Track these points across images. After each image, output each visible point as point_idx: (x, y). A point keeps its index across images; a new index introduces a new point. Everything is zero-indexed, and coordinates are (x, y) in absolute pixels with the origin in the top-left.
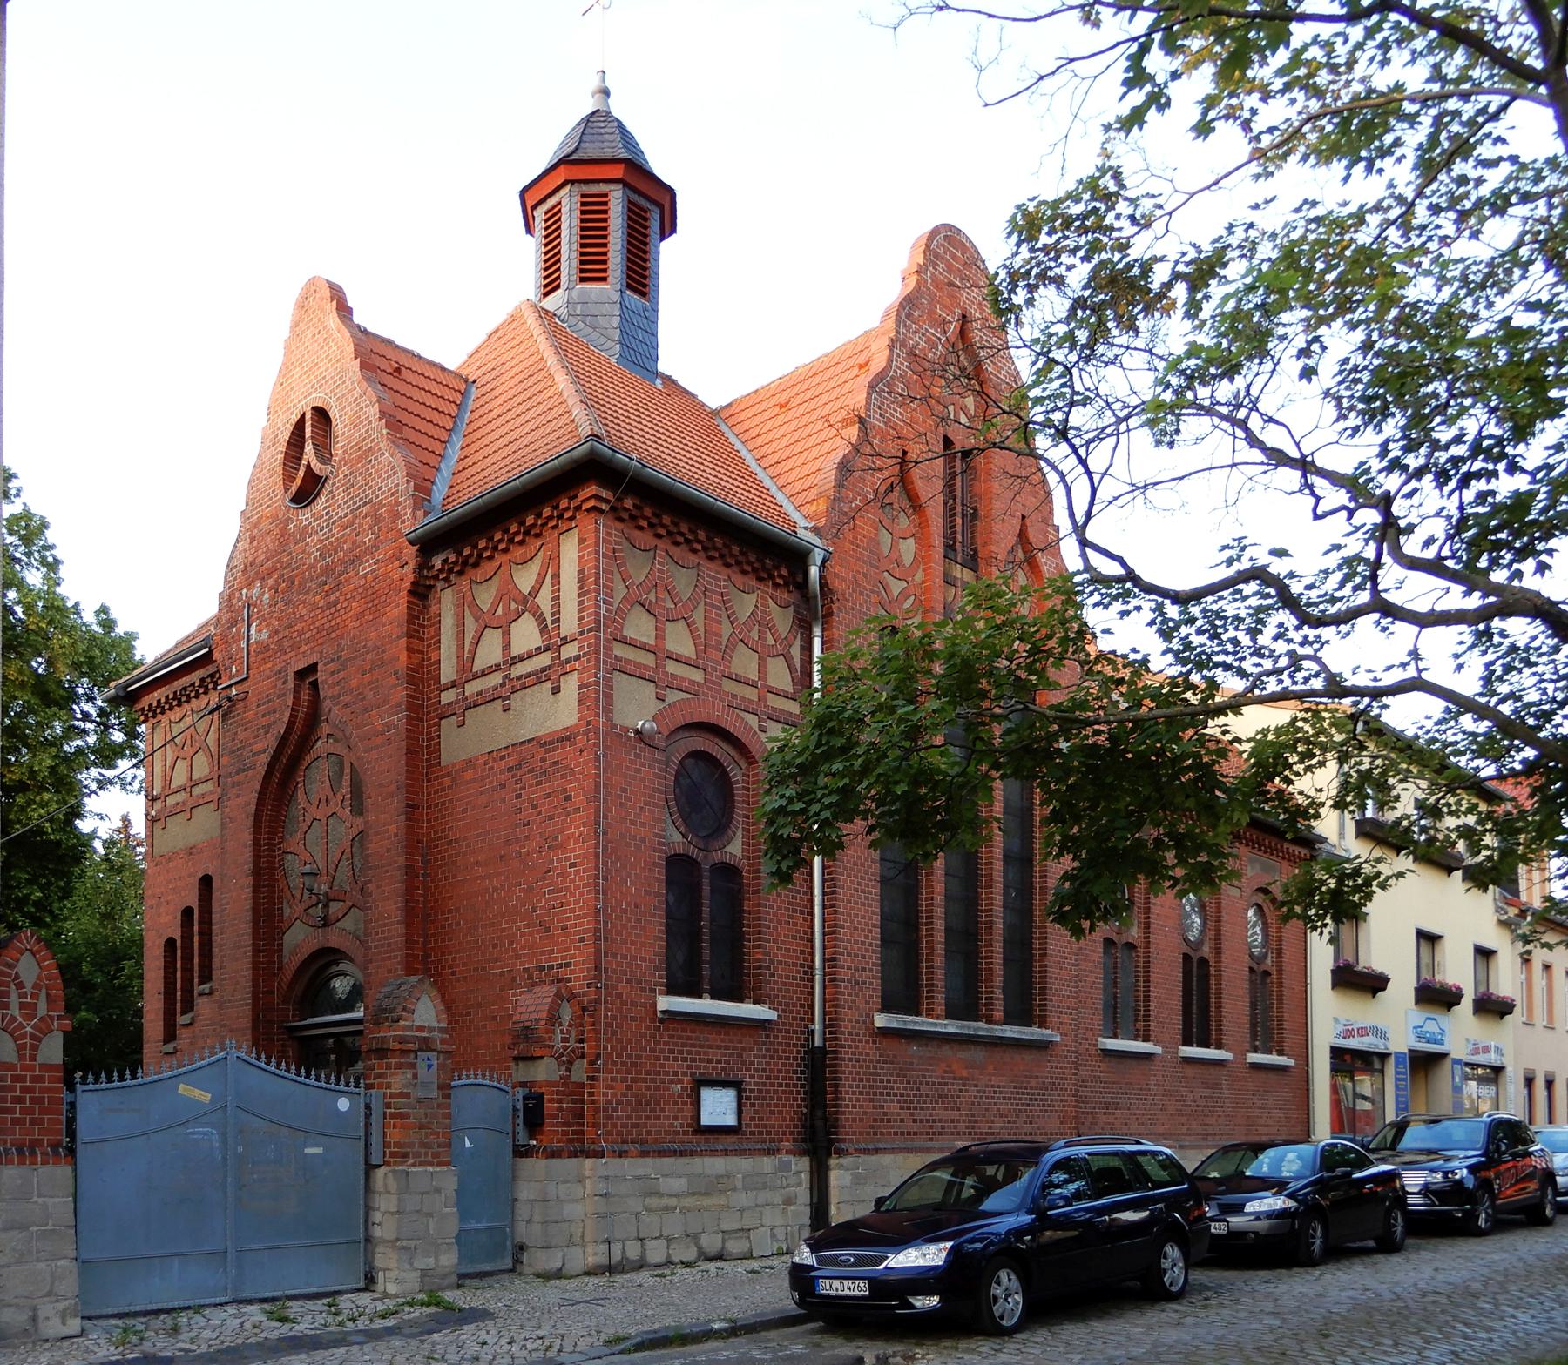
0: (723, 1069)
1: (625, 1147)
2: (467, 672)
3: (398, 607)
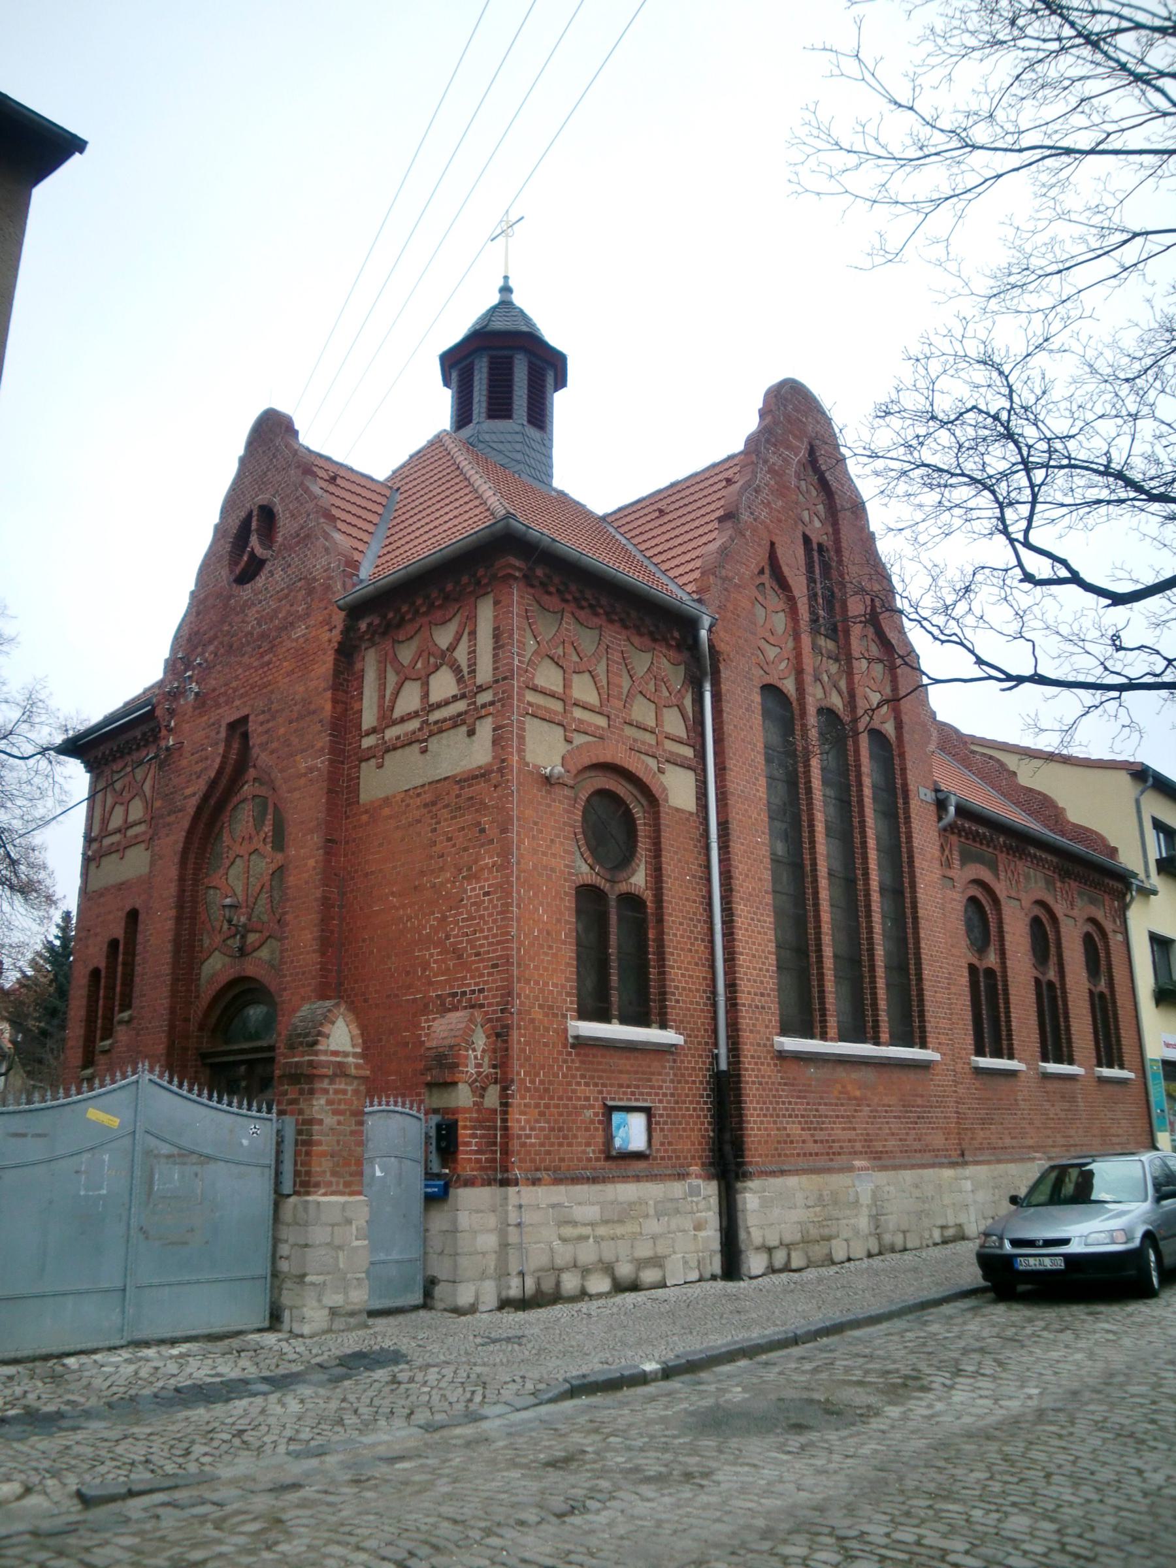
1: (539, 1175)
2: (387, 719)
3: (325, 665)
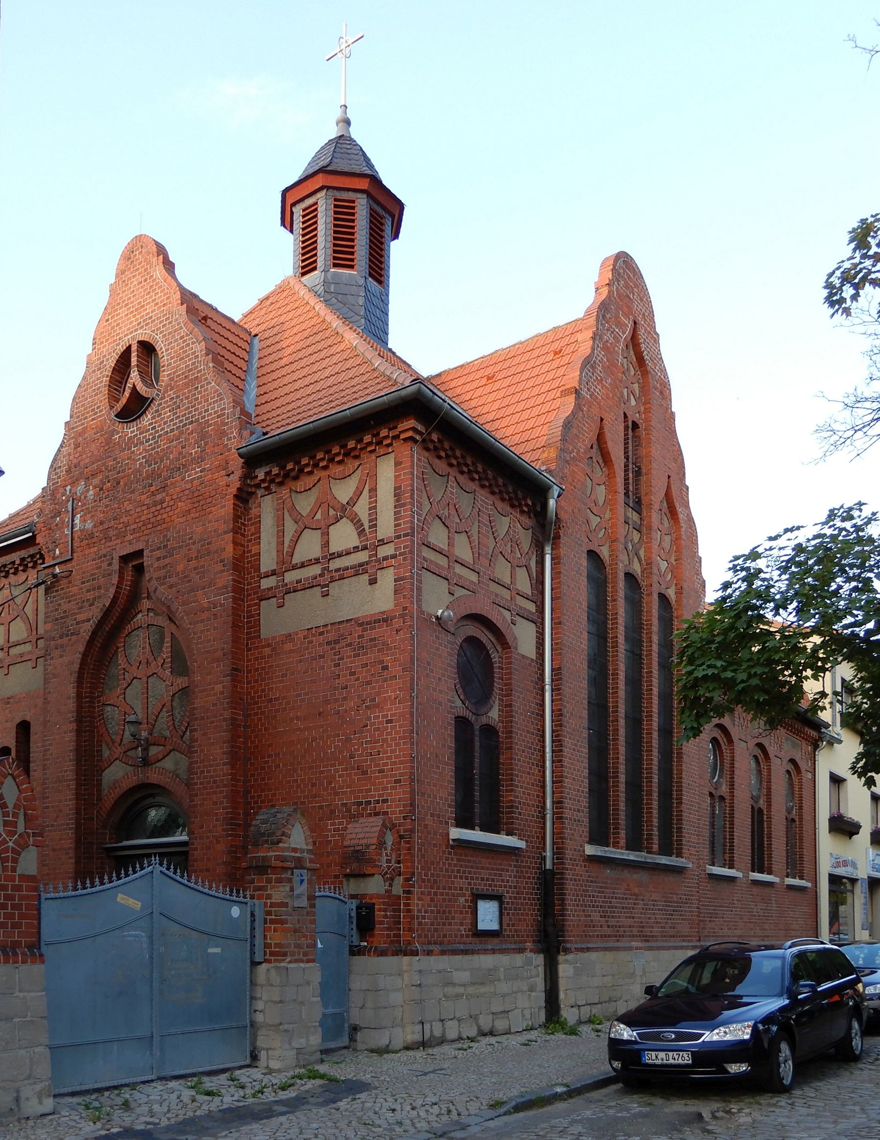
0: (490, 885)
1: (431, 947)
2: (286, 564)
3: (225, 507)
